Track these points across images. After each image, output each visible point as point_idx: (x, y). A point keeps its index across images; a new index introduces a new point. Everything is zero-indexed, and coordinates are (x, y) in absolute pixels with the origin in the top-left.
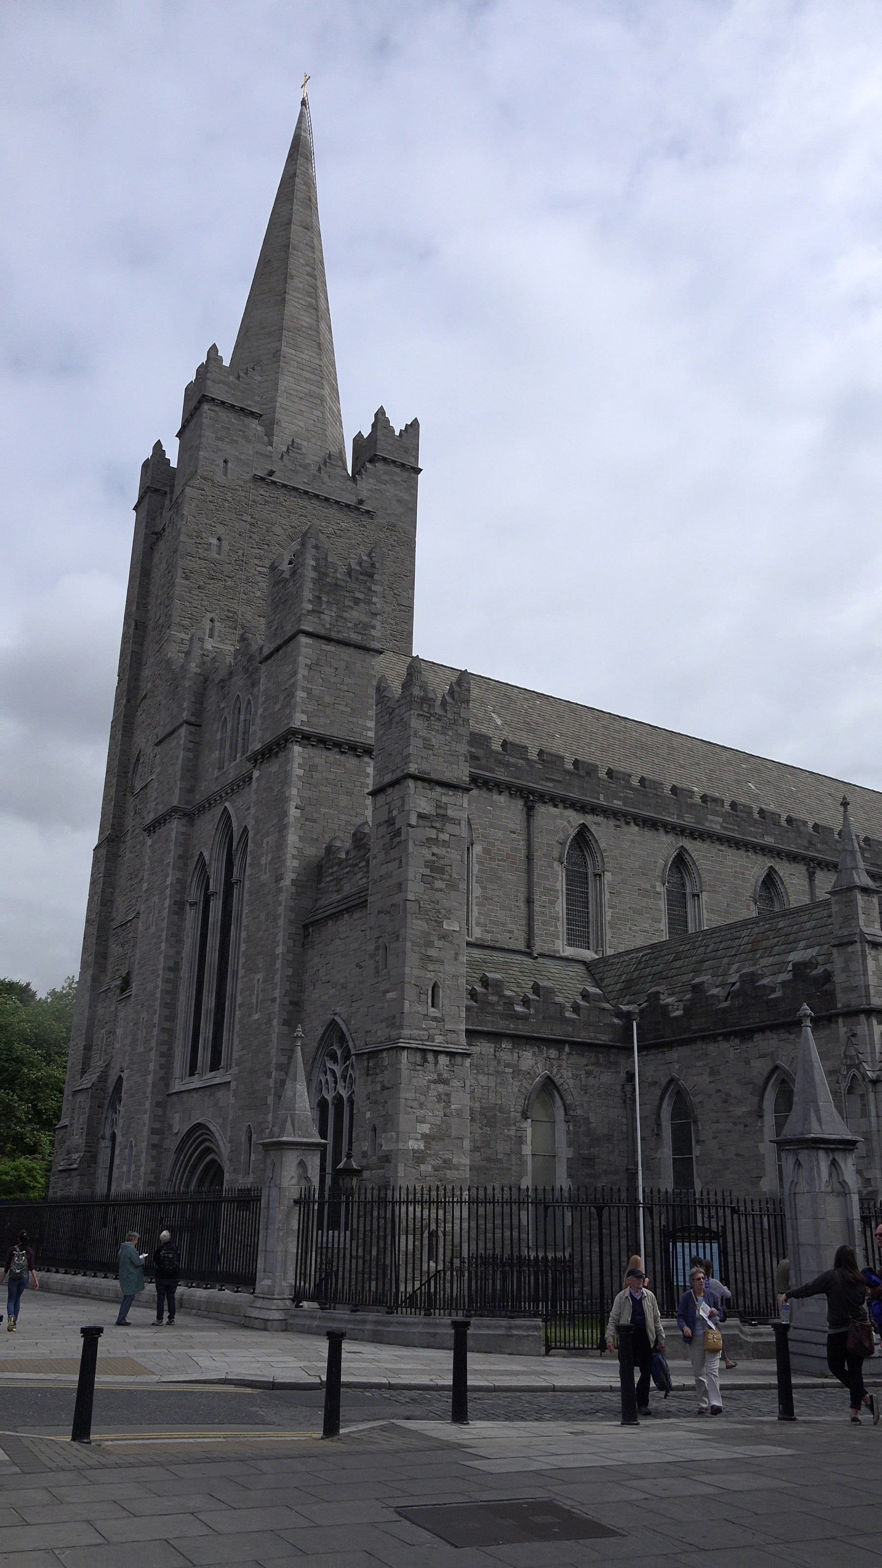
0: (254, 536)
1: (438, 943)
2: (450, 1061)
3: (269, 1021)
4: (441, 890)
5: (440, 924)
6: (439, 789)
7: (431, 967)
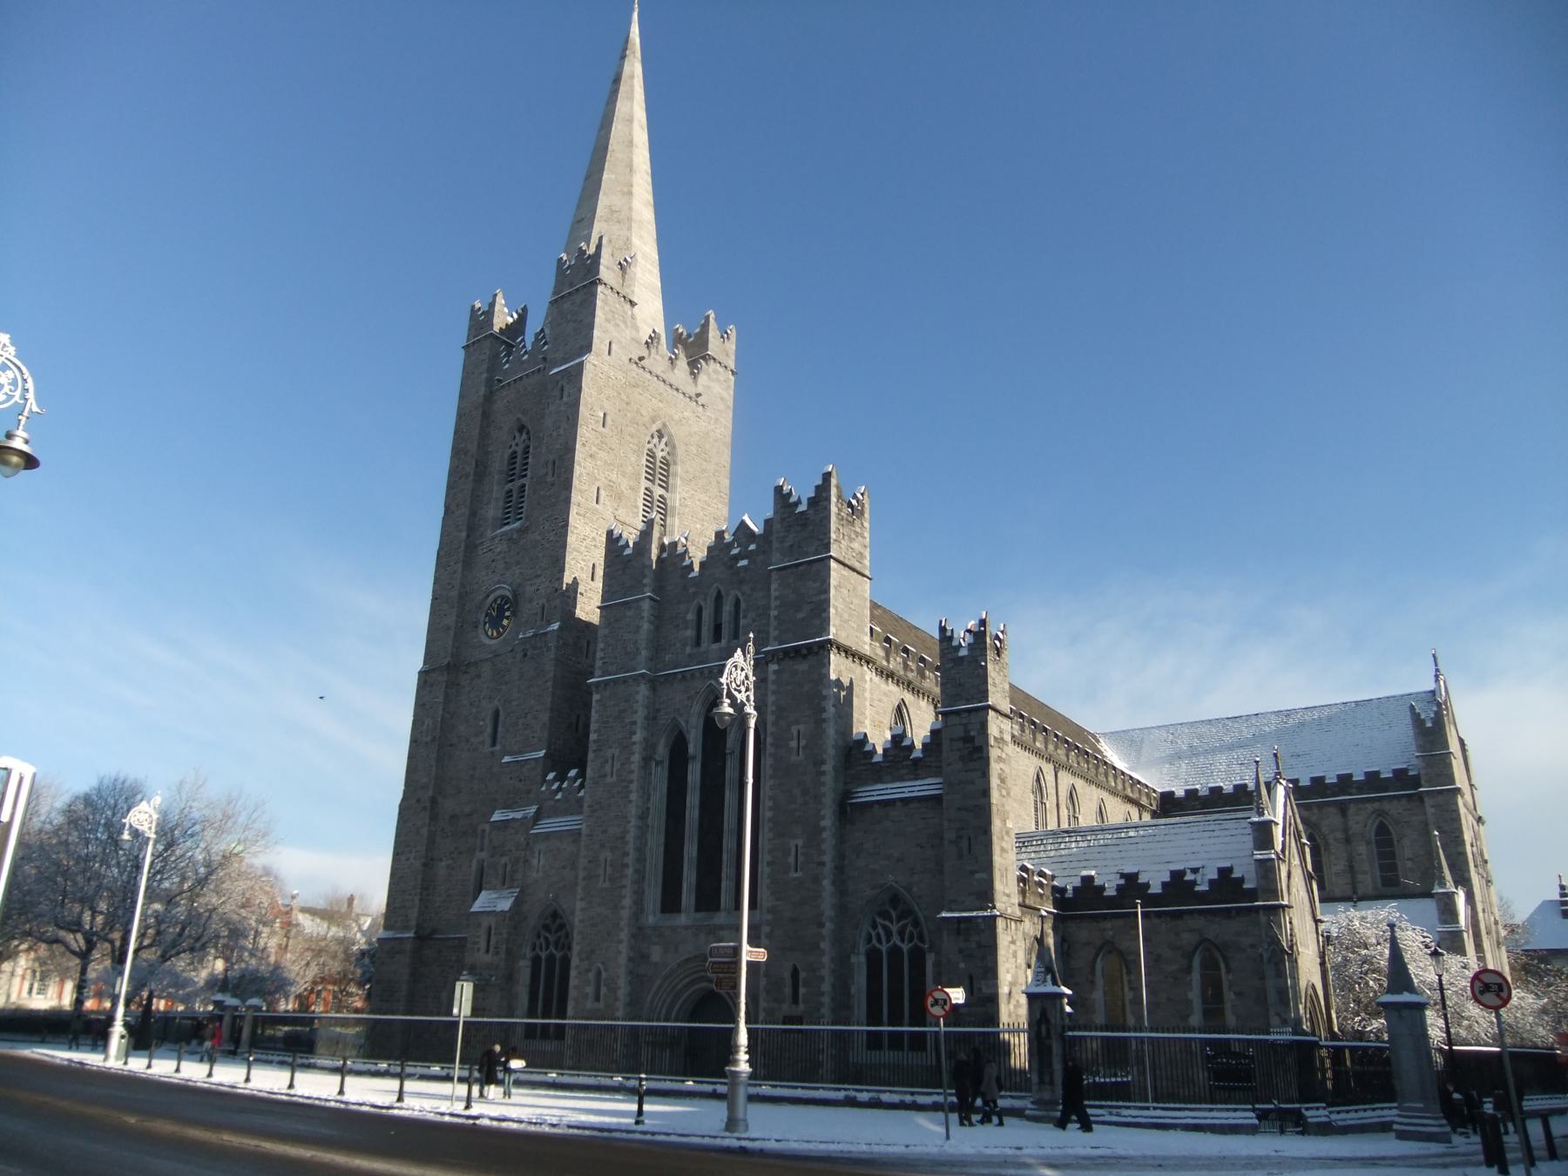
0: (629, 415)
3: (817, 880)
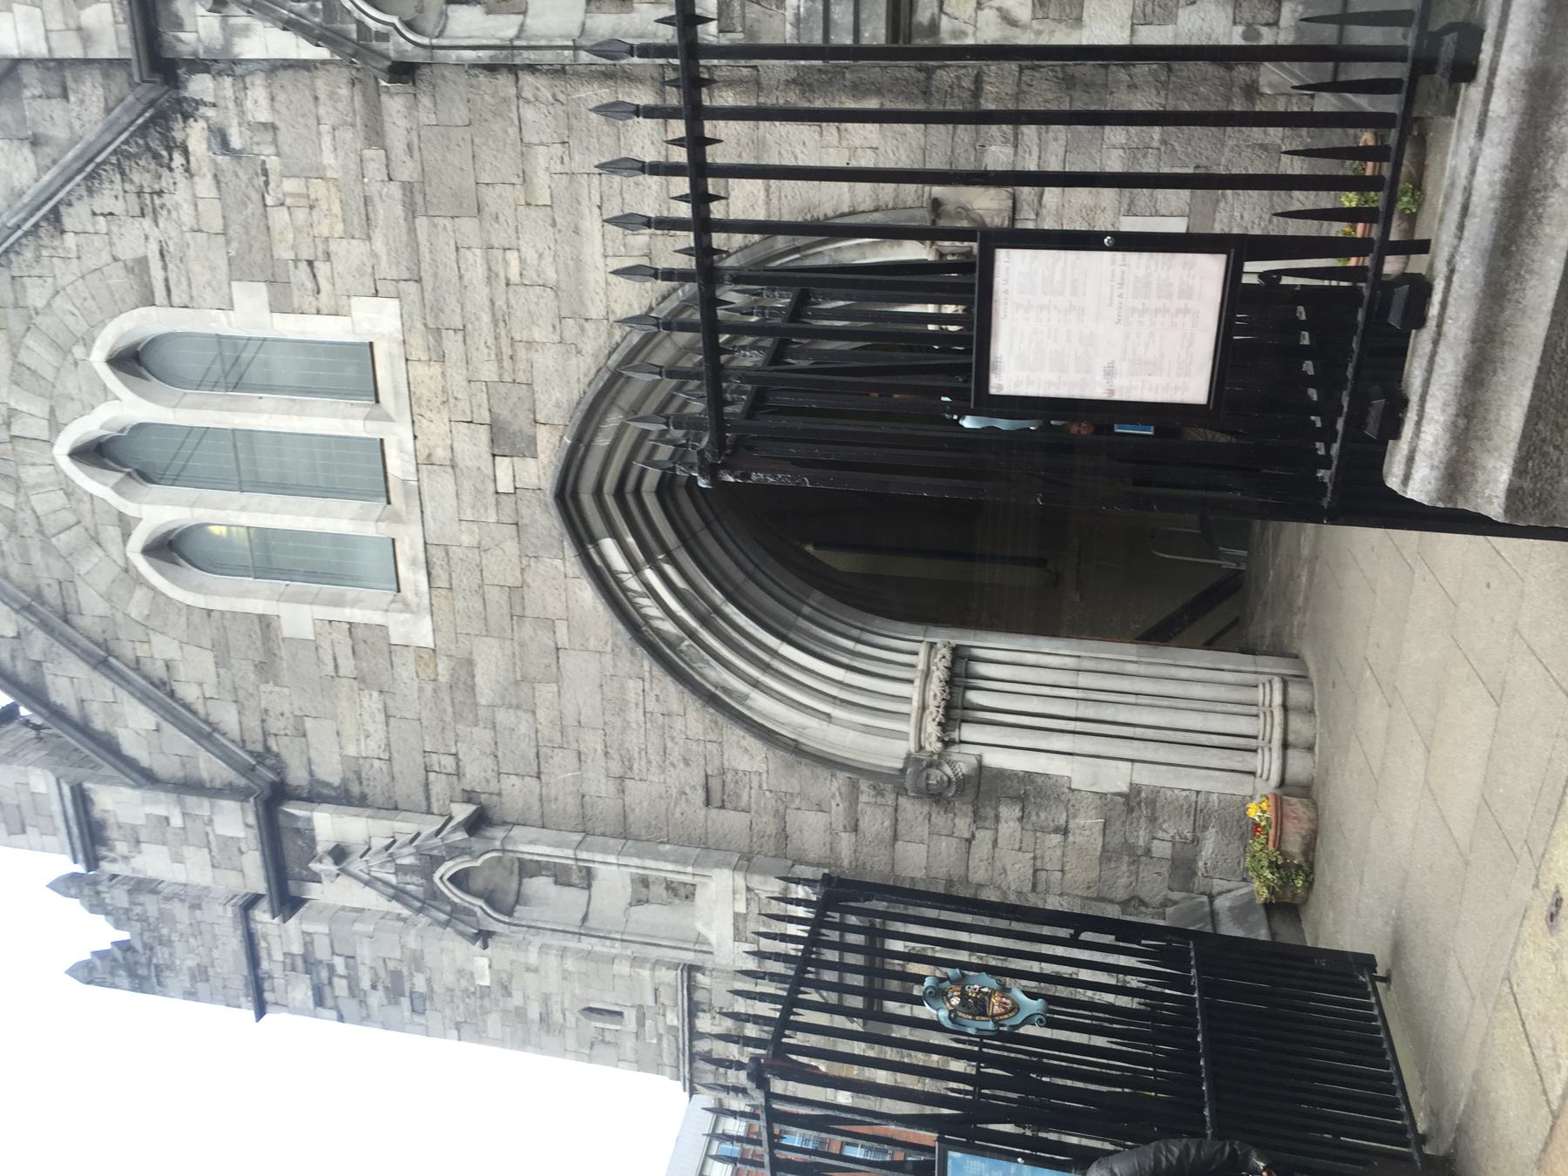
1: (517, 1000)
2: (704, 1011)
4: (429, 981)
5: (484, 992)
6: (265, 965)
7: (557, 1017)
